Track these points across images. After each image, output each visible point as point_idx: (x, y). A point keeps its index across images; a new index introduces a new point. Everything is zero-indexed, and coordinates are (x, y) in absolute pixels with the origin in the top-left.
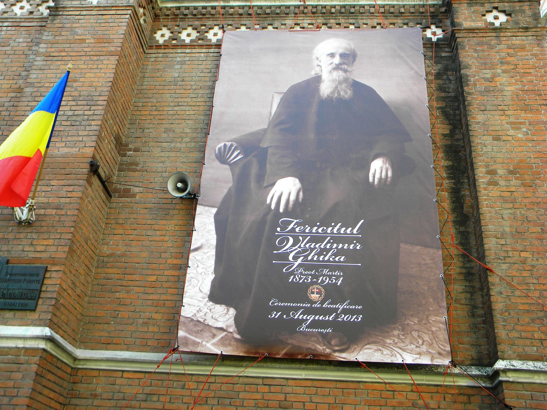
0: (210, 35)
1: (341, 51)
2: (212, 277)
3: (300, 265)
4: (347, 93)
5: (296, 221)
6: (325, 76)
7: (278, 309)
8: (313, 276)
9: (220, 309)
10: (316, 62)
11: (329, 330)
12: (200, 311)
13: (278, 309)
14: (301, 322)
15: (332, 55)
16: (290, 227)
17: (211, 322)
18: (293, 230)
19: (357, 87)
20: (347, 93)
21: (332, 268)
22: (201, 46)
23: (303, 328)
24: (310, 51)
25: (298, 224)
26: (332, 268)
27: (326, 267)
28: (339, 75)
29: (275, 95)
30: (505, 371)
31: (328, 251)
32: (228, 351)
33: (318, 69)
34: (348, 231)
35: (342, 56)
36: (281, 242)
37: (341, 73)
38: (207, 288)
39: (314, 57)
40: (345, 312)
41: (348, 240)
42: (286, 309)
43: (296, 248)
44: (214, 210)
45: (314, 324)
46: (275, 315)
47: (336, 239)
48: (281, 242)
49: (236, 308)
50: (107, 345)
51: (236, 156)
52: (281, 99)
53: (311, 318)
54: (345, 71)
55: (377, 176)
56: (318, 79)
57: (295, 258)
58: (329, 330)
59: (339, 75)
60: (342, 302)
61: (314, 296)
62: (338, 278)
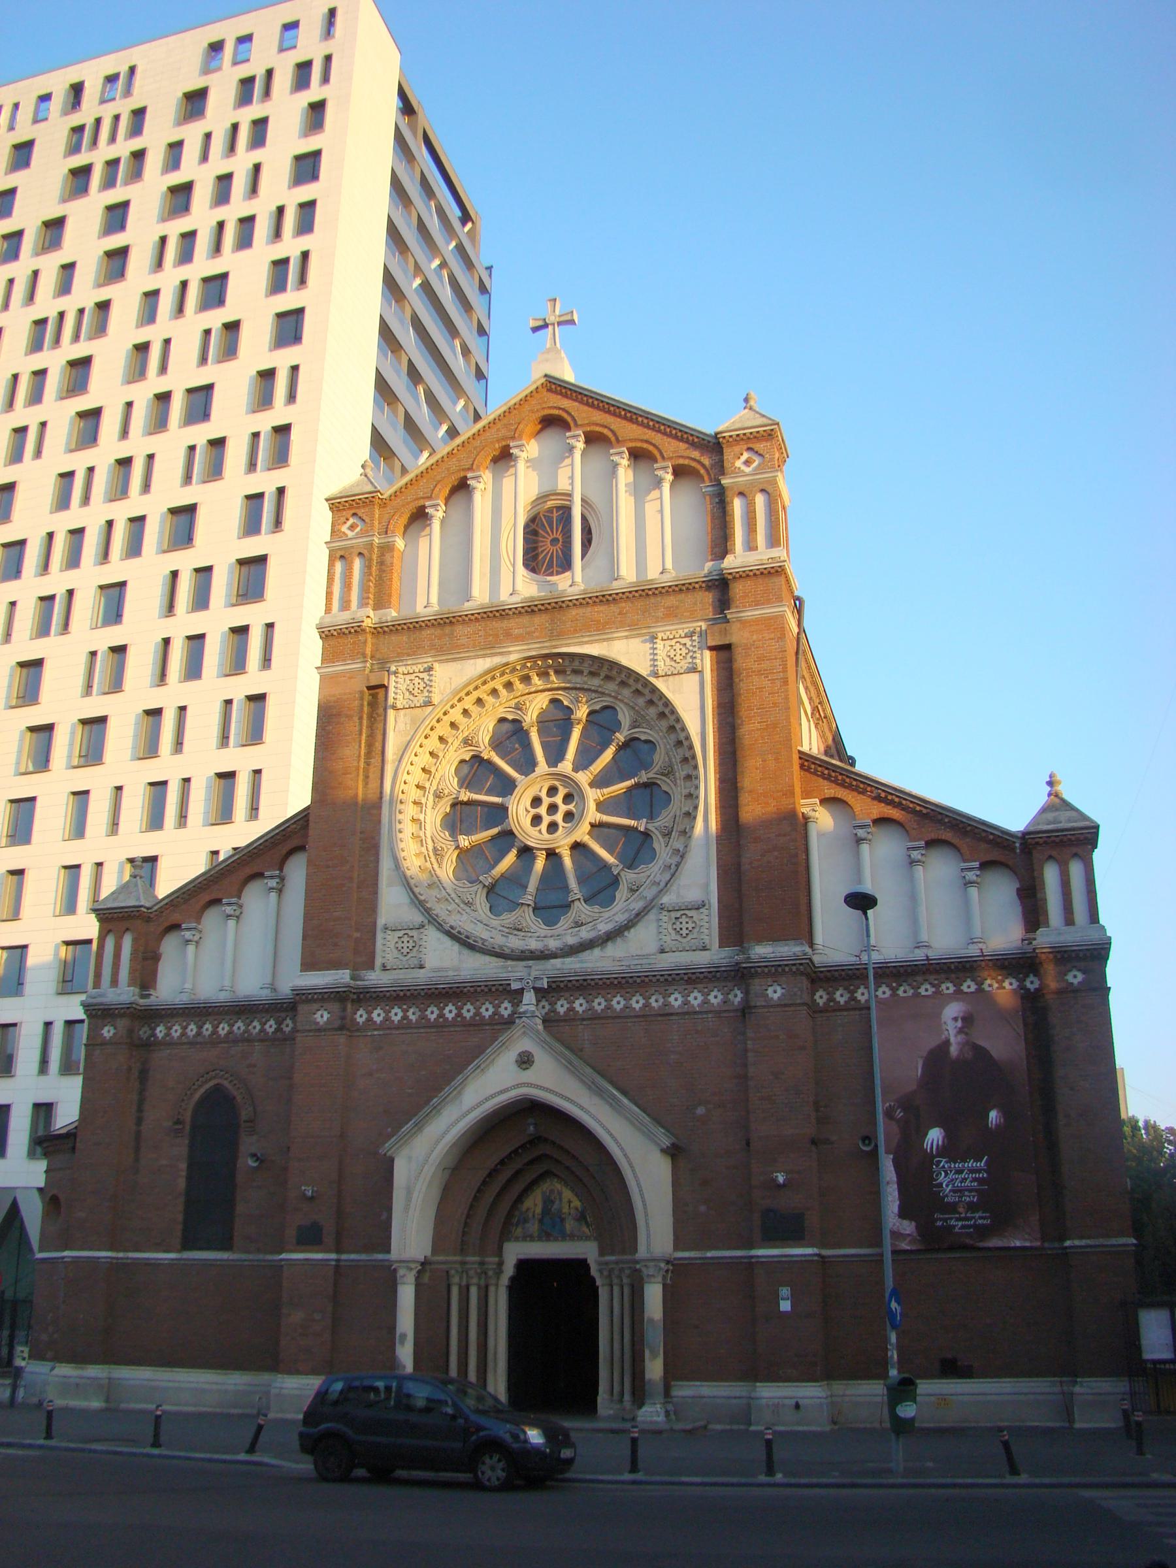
0: (858, 995)
1: (961, 1014)
2: (898, 1202)
3: (950, 1191)
4: (969, 1055)
5: (944, 1160)
6: (952, 1039)
7: (941, 1219)
8: (959, 1197)
9: (906, 1223)
10: (944, 1027)
11: (972, 1230)
12: (894, 1225)
13: (941, 1219)
14: (954, 1226)
15: (955, 1019)
16: (942, 1164)
17: (902, 1232)
18: (943, 1167)
19: (976, 1048)
20: (969, 1055)
21: (970, 1191)
22: (855, 1009)
23: (957, 1230)
24: (938, 1015)
25: (946, 1162)
26: (970, 1191)
27: (966, 1190)
28: (960, 1038)
29: (919, 1059)
30: (1071, 1247)
31: (966, 1179)
32: (914, 1248)
33: (946, 1033)
34: (978, 1165)
35: (964, 1019)
36: (937, 1175)
37: (963, 1036)
38: (896, 1210)
39: (943, 1021)
40: (981, 1218)
41: (978, 1171)
42: (945, 1220)
43: (947, 1180)
44: (891, 1156)
45: (963, 1227)
46: (939, 1223)
47: (971, 1171)
48: (937, 1175)
49: (915, 1221)
50: (840, 1246)
51: (899, 1114)
52: (924, 1062)
53: (960, 1223)
54: (966, 1034)
55: (994, 1122)
56: (947, 1043)
57: (947, 1186)
58: (972, 1230)
59: (960, 1038)
60: (978, 1212)
61: (961, 1210)
62: (974, 1197)
